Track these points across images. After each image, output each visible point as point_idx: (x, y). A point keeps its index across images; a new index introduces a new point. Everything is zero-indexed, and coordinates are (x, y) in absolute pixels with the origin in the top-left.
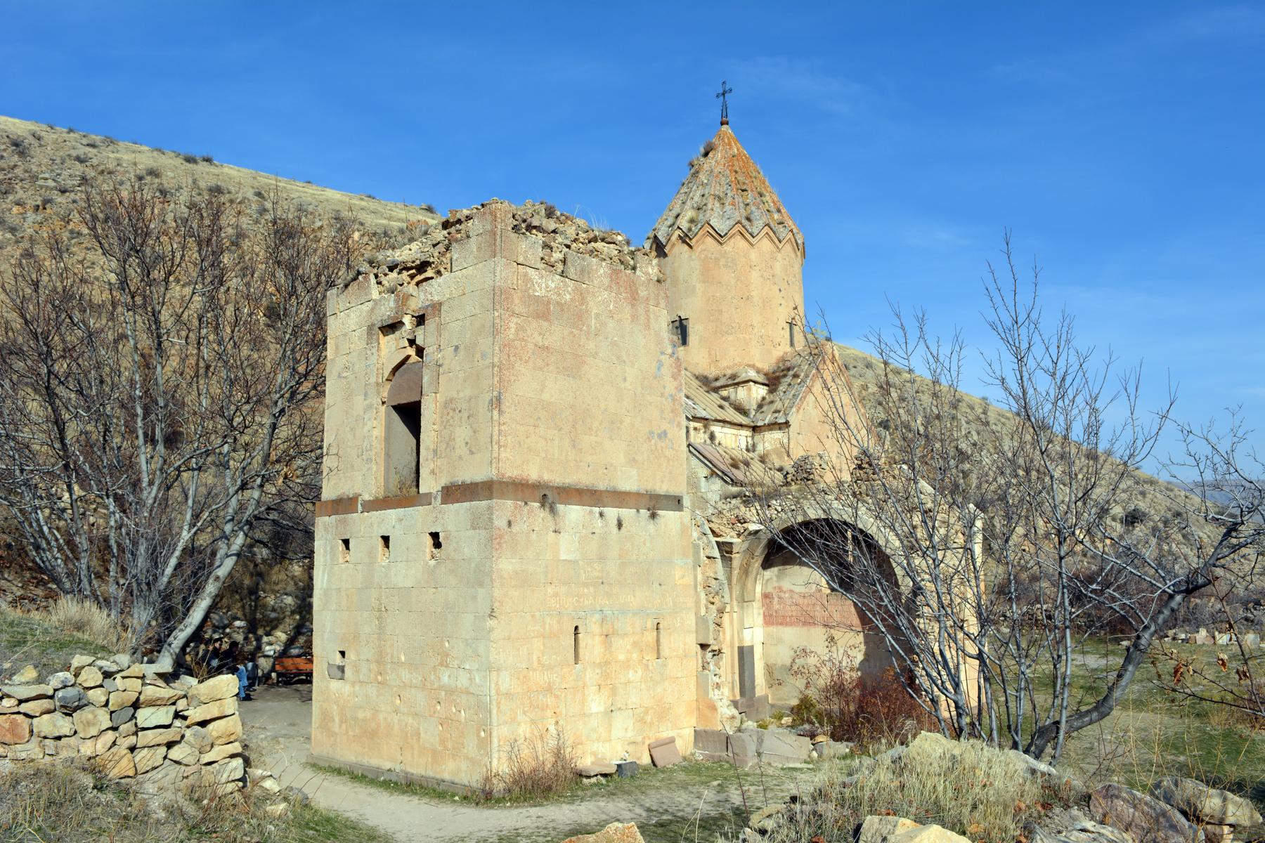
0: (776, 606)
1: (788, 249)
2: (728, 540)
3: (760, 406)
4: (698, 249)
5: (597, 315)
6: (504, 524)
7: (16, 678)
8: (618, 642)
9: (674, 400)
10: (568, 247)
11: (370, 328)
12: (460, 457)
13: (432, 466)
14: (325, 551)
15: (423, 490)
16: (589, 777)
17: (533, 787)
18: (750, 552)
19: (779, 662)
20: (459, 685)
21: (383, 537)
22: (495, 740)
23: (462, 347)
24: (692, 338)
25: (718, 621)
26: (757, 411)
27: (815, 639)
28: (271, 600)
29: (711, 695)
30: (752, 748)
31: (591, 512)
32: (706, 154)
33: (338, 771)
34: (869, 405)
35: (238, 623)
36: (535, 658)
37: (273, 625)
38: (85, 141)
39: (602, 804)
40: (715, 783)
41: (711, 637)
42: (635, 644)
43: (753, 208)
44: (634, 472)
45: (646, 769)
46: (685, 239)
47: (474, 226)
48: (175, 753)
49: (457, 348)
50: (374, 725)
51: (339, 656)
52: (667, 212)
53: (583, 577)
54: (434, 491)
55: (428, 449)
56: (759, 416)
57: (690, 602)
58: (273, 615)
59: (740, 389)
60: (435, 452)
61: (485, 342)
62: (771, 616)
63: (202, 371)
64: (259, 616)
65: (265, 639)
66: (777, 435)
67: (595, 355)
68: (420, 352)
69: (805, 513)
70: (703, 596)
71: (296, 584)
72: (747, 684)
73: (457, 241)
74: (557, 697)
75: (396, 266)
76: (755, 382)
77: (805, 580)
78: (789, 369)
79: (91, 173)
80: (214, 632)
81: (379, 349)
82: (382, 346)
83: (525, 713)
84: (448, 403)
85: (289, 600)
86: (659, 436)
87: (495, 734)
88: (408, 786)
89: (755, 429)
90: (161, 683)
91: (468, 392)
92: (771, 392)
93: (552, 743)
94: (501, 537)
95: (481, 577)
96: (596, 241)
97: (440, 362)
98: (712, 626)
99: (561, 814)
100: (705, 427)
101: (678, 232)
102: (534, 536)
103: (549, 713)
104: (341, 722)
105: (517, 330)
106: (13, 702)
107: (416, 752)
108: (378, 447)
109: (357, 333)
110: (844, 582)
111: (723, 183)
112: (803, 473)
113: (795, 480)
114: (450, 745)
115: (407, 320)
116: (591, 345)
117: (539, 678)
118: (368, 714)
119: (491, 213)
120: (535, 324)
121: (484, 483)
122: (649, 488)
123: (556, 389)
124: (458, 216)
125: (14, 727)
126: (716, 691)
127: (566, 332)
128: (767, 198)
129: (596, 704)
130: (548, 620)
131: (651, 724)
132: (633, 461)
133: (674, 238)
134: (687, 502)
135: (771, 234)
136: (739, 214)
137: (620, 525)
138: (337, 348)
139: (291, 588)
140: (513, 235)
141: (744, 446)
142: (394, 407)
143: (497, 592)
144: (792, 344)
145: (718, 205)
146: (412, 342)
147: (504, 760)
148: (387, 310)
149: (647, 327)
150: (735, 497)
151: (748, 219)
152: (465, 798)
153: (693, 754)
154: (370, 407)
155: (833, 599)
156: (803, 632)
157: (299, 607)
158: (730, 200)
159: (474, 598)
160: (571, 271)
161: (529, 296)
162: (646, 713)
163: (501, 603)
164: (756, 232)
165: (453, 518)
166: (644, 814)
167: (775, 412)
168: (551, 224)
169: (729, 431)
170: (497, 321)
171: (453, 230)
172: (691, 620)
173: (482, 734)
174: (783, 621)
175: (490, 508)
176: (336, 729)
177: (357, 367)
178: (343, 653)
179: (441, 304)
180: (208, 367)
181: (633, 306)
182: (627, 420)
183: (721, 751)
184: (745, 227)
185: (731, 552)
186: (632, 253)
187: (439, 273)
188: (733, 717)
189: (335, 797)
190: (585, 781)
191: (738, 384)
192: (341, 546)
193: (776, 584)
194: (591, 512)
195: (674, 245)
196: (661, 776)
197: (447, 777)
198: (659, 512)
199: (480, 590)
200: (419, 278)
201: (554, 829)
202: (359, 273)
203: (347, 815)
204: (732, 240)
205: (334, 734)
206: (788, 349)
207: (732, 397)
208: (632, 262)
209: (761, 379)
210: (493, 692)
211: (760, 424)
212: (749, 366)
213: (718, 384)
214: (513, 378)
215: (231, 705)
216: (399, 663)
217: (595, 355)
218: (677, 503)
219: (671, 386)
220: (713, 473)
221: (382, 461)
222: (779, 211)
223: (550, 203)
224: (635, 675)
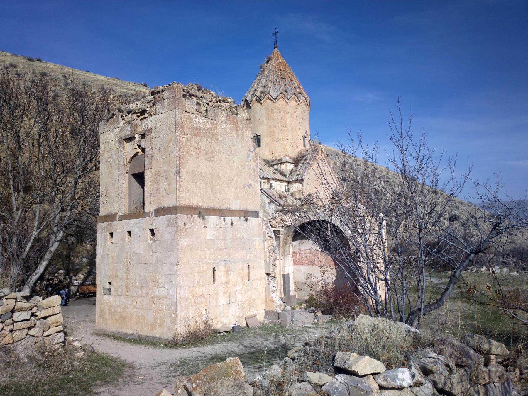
0: (298, 257)
1: (303, 104)
2: (278, 229)
3: (291, 173)
4: (264, 105)
5: (221, 134)
6: (183, 224)
8: (231, 274)
9: (254, 171)
10: (208, 104)
11: (120, 139)
12: (163, 196)
13: (150, 200)
14: (102, 238)
15: (146, 211)
16: (220, 333)
17: (195, 338)
18: (287, 234)
19: (300, 281)
20: (163, 295)
21: (128, 231)
22: (179, 319)
23: (162, 148)
24: (262, 144)
25: (274, 264)
26: (290, 175)
27: (316, 271)
28: (76, 261)
29: (271, 295)
30: (289, 318)
31: (220, 219)
32: (268, 62)
34: (337, 171)
35: (61, 271)
36: (196, 282)
37: (77, 272)
39: (225, 345)
40: (274, 334)
41: (271, 271)
42: (239, 274)
43: (288, 87)
44: (238, 201)
45: (244, 328)
46: (259, 100)
47: (166, 94)
49: (160, 149)
50: (124, 314)
51: (108, 284)
52: (250, 88)
53: (217, 246)
55: (148, 193)
57: (262, 256)
58: (77, 267)
59: (282, 165)
60: (151, 194)
61: (172, 147)
62: (296, 261)
63: (41, 158)
65: (74, 278)
67: (220, 152)
68: (143, 150)
69: (310, 218)
70: (267, 253)
71: (88, 253)
72: (287, 290)
73: (158, 101)
74: (206, 298)
75: (131, 112)
76: (289, 162)
78: (303, 157)
80: (50, 276)
81: (124, 149)
82: (126, 147)
84: (157, 173)
86: (249, 186)
87: (179, 316)
89: (289, 182)
91: (165, 168)
92: (295, 166)
93: (204, 318)
94: (181, 230)
95: (172, 248)
96: (220, 102)
97: (153, 155)
98: (272, 266)
99: (208, 350)
100: (268, 182)
101: (256, 97)
102: (195, 229)
103: (203, 305)
104: (109, 313)
105: (186, 141)
108: (125, 192)
110: (326, 246)
111: (275, 75)
112: (309, 201)
113: (306, 204)
114: (159, 321)
115: (137, 136)
116: (219, 148)
118: (122, 310)
119: (173, 89)
120: (194, 138)
121: (173, 207)
122: (244, 208)
124: (158, 89)
126: (274, 294)
127: (208, 142)
128: (294, 82)
129: (223, 301)
131: (246, 308)
132: (237, 197)
133: (254, 100)
134: (260, 214)
137: (232, 224)
138: (105, 148)
139: (86, 254)
140: (183, 99)
141: (284, 190)
142: (132, 175)
143: (180, 254)
144: (304, 146)
145: (273, 85)
146: (139, 146)
148: (127, 131)
149: (243, 140)
150: (281, 211)
151: (286, 91)
152: (166, 345)
153: (264, 321)
154: (121, 174)
155: (323, 254)
156: (309, 268)
157: (89, 263)
158: (278, 83)
160: (210, 115)
161: (191, 126)
162: (244, 304)
164: (289, 97)
165: (160, 223)
166: (244, 349)
167: (297, 175)
168: (200, 94)
169: (278, 183)
170: (178, 137)
171: (156, 96)
172: (262, 263)
173: (173, 316)
175: (176, 218)
176: (107, 317)
177: (114, 157)
178: (110, 283)
179: (152, 129)
180: (43, 157)
181: (237, 130)
182: (235, 179)
183: (276, 319)
184: (284, 95)
185: (279, 234)
186: (236, 107)
187: (150, 115)
188: (281, 305)
189: (107, 348)
190: (218, 334)
191: (282, 163)
192: (109, 236)
193: (298, 248)
194: (220, 219)
195: (254, 103)
196: (251, 331)
197: (157, 335)
199: (172, 254)
200: (141, 117)
201: (205, 357)
202: (114, 115)
203: (112, 355)
204: (279, 101)
206: (303, 148)
207: (279, 169)
208: (236, 111)
209: (291, 161)
210: (178, 297)
211: (291, 180)
212: (286, 155)
213: (273, 163)
214: (185, 162)
215: (58, 309)
216: (136, 287)
218: (256, 214)
219: (253, 165)
220: (271, 201)
222: (299, 88)
223: (199, 85)
224: (239, 288)
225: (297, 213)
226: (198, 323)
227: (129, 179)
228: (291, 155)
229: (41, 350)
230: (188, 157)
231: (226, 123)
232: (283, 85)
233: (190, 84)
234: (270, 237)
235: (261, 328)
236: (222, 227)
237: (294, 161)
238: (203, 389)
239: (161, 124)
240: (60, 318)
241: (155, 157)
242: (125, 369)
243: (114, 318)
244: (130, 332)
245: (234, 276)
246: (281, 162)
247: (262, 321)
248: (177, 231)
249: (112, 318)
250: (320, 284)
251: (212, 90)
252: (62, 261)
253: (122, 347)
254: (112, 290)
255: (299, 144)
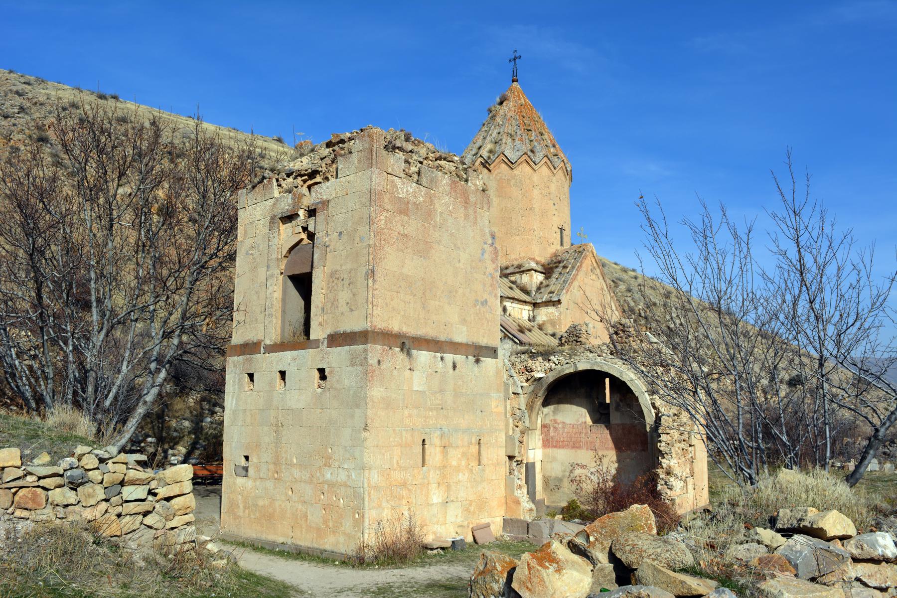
0: (552, 434)
1: (560, 174)
3: (539, 288)
5: (441, 213)
7: (36, 461)
8: (452, 452)
9: (493, 278)
10: (421, 163)
11: (273, 218)
12: (342, 314)
13: (320, 320)
14: (234, 382)
15: (311, 338)
16: (432, 549)
17: (394, 555)
18: (534, 393)
19: (554, 475)
20: (339, 480)
21: (281, 372)
22: (367, 521)
23: (345, 233)
25: (521, 439)
26: (536, 292)
27: (585, 456)
28: (173, 423)
30: (546, 531)
31: (435, 357)
32: (501, 103)
33: (243, 544)
35: (149, 439)
36: (395, 461)
37: (175, 442)
38: (22, 80)
39: (445, 567)
41: (517, 451)
43: (536, 144)
44: (465, 329)
45: (470, 545)
47: (356, 145)
48: (149, 520)
49: (341, 234)
50: (271, 510)
51: (244, 459)
54: (321, 338)
55: (317, 307)
56: (538, 296)
57: (502, 425)
58: (175, 434)
59: (524, 275)
60: (323, 309)
61: (363, 230)
62: (548, 440)
63: (140, 248)
64: (164, 434)
65: (170, 452)
66: (551, 309)
67: (439, 242)
68: (311, 236)
69: (576, 366)
70: (511, 420)
71: (191, 412)
73: (341, 156)
74: (409, 490)
76: (536, 271)
77: (576, 415)
78: (560, 262)
79: (27, 104)
80: (132, 445)
82: (281, 231)
83: (387, 501)
84: (333, 274)
85: (187, 424)
86: (482, 303)
87: (366, 516)
88: (299, 554)
89: (535, 305)
90: (139, 468)
91: (349, 266)
92: (547, 278)
93: (406, 524)
94: (373, 371)
95: (358, 401)
96: (440, 160)
97: (328, 244)
98: (517, 443)
99: (420, 574)
101: (480, 159)
102: (395, 372)
103: (404, 502)
104: (245, 508)
105: (386, 222)
106: (34, 478)
107: (304, 530)
108: (278, 306)
109: (261, 222)
110: (601, 415)
112: (574, 337)
114: (331, 524)
115: (301, 213)
116: (436, 235)
117: (397, 476)
118: (267, 502)
119: (369, 136)
120: (398, 218)
121: (361, 332)
122: (475, 341)
123: (412, 266)
124: (342, 137)
125: (35, 496)
126: (519, 491)
127: (419, 225)
128: (546, 137)
129: (436, 497)
130: (404, 433)
131: (474, 513)
132: (464, 321)
133: (478, 163)
135: (549, 163)
136: (526, 148)
137: (454, 367)
138: (246, 232)
139: (187, 415)
141: (526, 318)
143: (370, 412)
144: (562, 244)
145: (510, 140)
146: (305, 229)
147: (373, 535)
148: (286, 204)
149: (475, 224)
150: (524, 353)
151: (532, 151)
152: (343, 563)
153: (502, 536)
154: (272, 276)
155: (594, 429)
156: (578, 450)
158: (519, 137)
159: (352, 416)
160: (424, 181)
161: (395, 197)
162: (471, 505)
163: (372, 420)
164: (537, 161)
165: (336, 359)
167: (550, 293)
168: (409, 147)
169: (517, 306)
170: (373, 214)
171: (336, 148)
172: (502, 439)
173: (357, 516)
174: (557, 445)
175: (365, 351)
176: (241, 513)
178: (247, 458)
180: (144, 246)
181: (466, 208)
182: (461, 291)
183: (523, 533)
186: (465, 169)
187: (327, 179)
188: (531, 510)
189: (251, 562)
190: (429, 552)
191: (523, 272)
192: (247, 379)
193: (552, 418)
197: (328, 547)
198: (482, 359)
199: (357, 410)
201: (416, 583)
202: (264, 178)
203: (261, 573)
204: (520, 167)
205: (239, 517)
206: (559, 247)
207: (519, 281)
208: (465, 176)
209: (539, 268)
210: (366, 485)
212: (531, 259)
213: (508, 271)
215: (188, 486)
216: (292, 465)
217: (439, 242)
218: (493, 352)
220: (506, 336)
221: (279, 315)
222: (554, 146)
223: (408, 131)
224: (463, 477)
225: (552, 358)
226: (398, 531)
227: (284, 283)
228: (538, 259)
229: (164, 549)
230: (387, 248)
231: (449, 194)
232: (528, 141)
233: (392, 130)
234: (514, 393)
235: (498, 546)
236: (439, 371)
237: (545, 269)
238: (606, 545)
239: (344, 193)
240: (190, 502)
241: (331, 247)
242: (292, 592)
243: (252, 516)
244: (281, 540)
245: (455, 457)
246: (521, 270)
247: (498, 535)
248: (366, 373)
249: (249, 515)
250: (595, 479)
251: (427, 141)
252: (152, 422)
253: (271, 563)
254: (249, 469)
255: (552, 240)
